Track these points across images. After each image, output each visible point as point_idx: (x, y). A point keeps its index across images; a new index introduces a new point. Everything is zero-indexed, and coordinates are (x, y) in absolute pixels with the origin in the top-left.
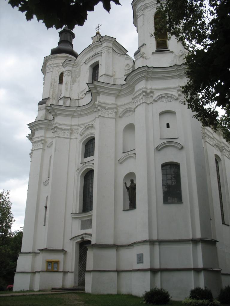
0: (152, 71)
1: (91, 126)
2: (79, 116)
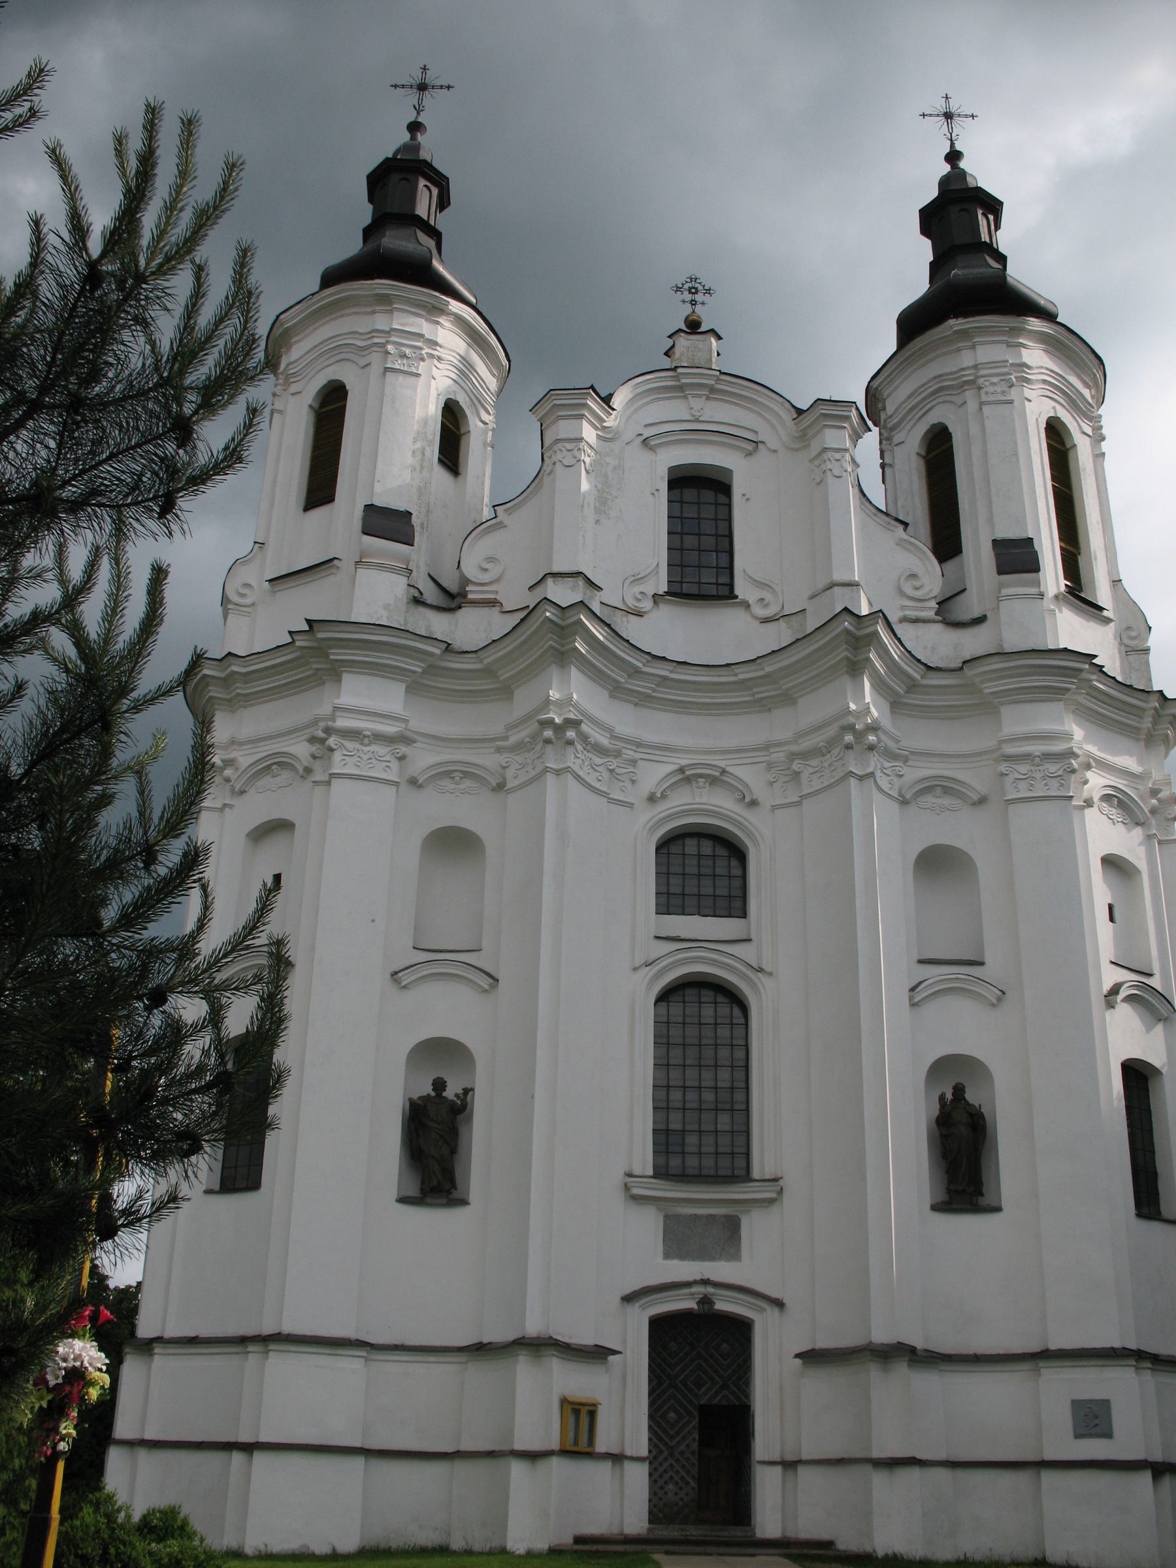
1: (717, 774)
2: (643, 700)
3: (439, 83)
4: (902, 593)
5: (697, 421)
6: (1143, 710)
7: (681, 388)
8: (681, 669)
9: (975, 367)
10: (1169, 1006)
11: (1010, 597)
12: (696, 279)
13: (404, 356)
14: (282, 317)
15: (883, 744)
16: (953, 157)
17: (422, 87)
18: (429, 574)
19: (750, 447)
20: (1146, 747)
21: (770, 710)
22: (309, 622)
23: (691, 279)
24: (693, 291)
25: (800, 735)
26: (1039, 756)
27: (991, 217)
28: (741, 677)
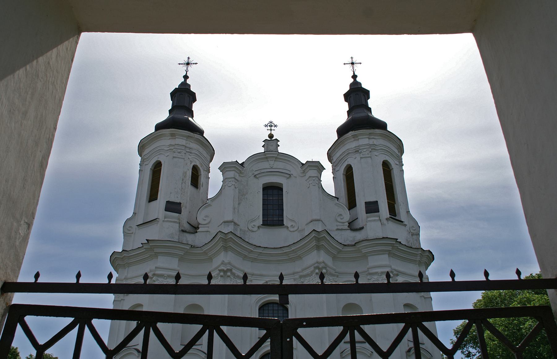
0: (398, 247)
2: (254, 260)
3: (193, 62)
4: (337, 221)
5: (272, 168)
6: (417, 254)
7: (267, 158)
8: (266, 249)
9: (359, 146)
10: (430, 355)
11: (371, 221)
12: (272, 122)
13: (179, 153)
14: (142, 140)
15: (329, 272)
16: (355, 77)
17: (188, 64)
18: (187, 222)
19: (288, 176)
20: (419, 266)
21: (294, 261)
22: (147, 240)
23: (270, 122)
24: (271, 126)
25: (304, 270)
26: (380, 273)
27: (366, 96)
28: (285, 251)
